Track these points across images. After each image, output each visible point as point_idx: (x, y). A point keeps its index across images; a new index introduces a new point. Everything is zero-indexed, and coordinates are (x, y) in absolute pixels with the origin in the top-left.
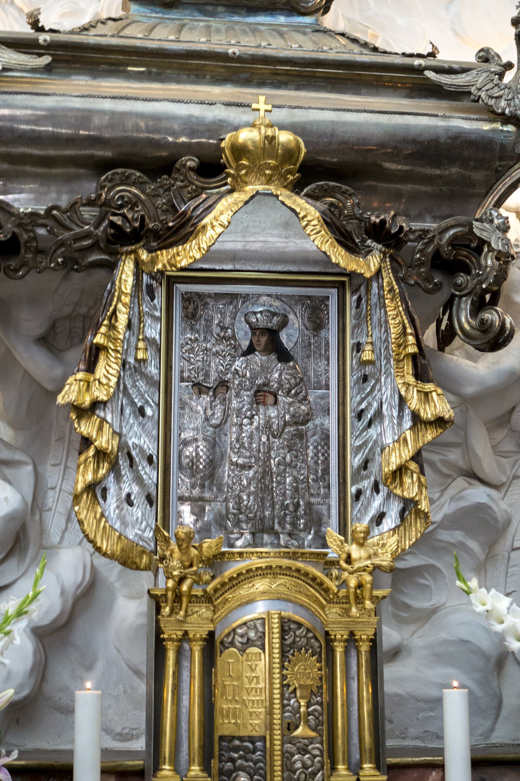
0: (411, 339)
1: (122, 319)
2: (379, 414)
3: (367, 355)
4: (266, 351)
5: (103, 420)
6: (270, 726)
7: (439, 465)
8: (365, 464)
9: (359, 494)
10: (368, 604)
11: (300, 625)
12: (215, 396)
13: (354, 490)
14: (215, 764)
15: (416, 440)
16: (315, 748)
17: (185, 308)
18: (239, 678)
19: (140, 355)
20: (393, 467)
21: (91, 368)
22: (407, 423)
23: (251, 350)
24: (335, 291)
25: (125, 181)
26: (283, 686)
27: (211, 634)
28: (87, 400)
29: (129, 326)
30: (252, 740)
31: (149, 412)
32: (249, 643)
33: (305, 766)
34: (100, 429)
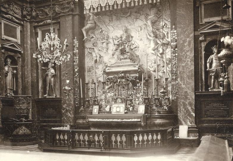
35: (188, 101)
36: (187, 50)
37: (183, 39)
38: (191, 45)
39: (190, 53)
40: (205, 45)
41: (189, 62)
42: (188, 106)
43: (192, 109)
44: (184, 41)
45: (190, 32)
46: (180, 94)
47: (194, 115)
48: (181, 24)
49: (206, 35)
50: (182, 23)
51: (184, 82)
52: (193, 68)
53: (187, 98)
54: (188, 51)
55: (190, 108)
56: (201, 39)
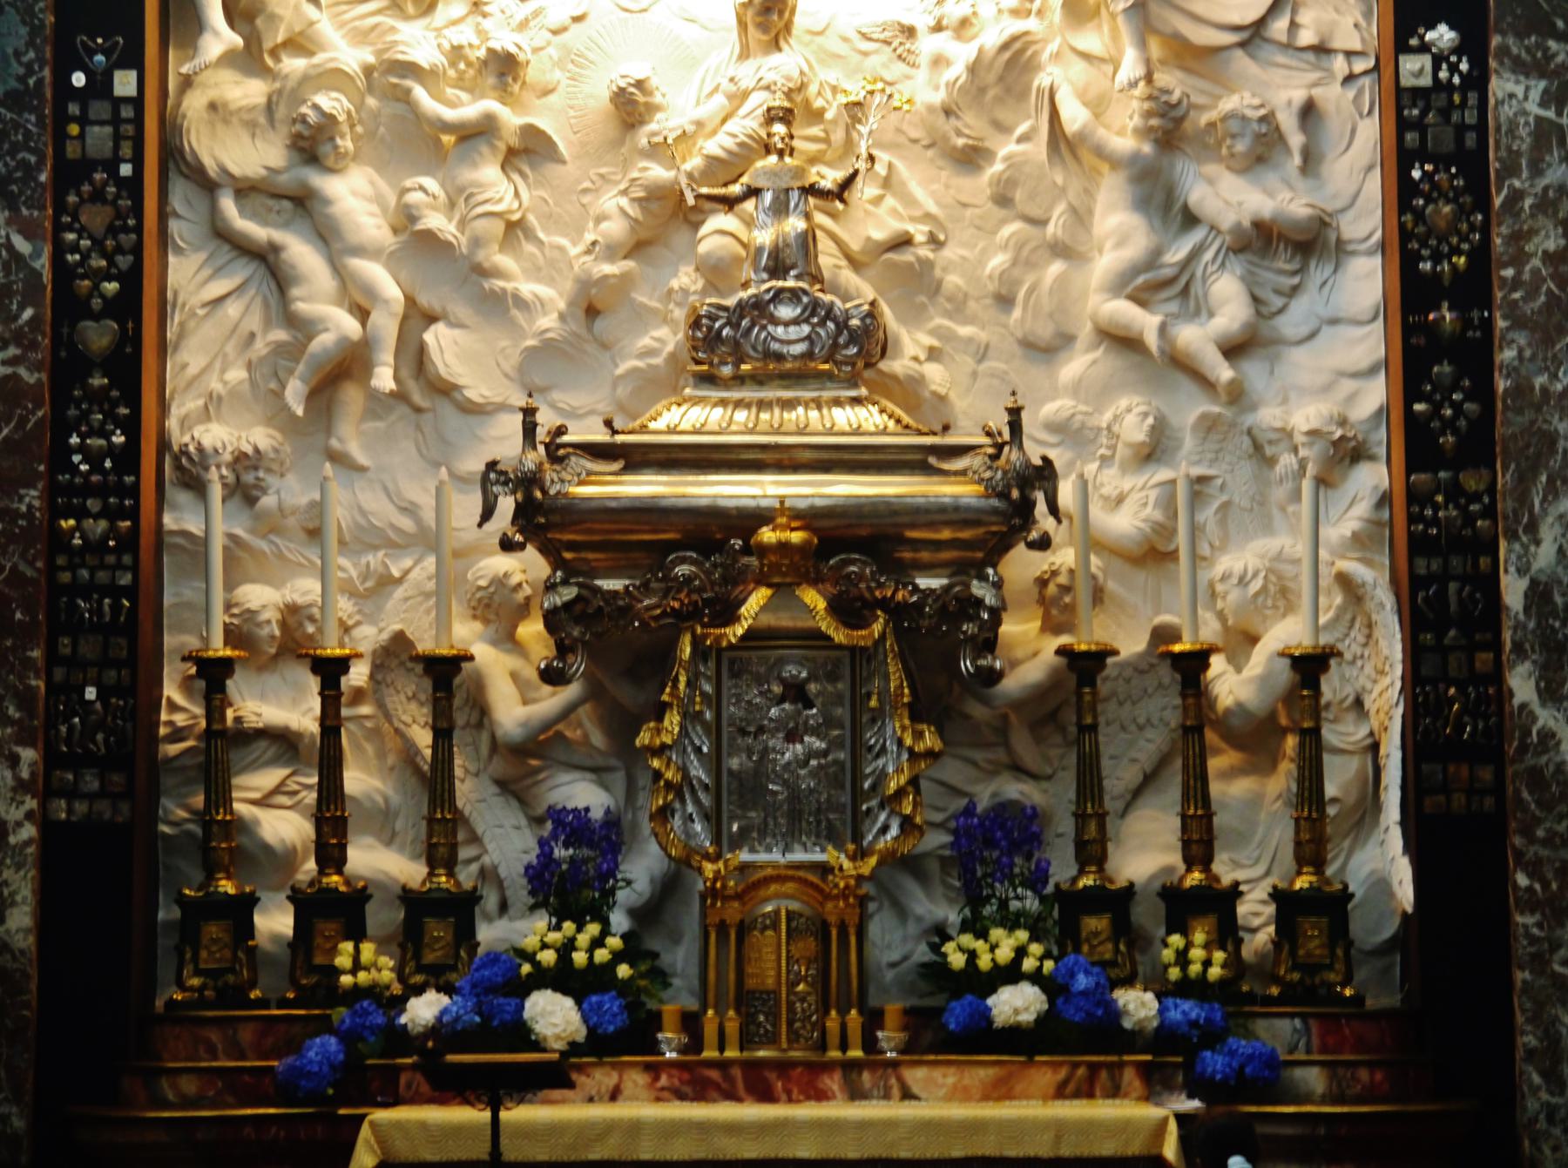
0: (906, 691)
1: (683, 679)
2: (884, 746)
3: (873, 703)
4: (793, 702)
5: (670, 759)
6: (779, 983)
7: (983, 764)
8: (874, 787)
9: (869, 810)
10: (851, 900)
11: (801, 915)
12: (755, 738)
13: (864, 807)
14: (743, 1009)
15: (911, 768)
16: (811, 999)
17: (731, 669)
18: (760, 951)
19: (697, 708)
20: (891, 792)
21: (660, 719)
22: (905, 756)
23: (781, 700)
24: (846, 653)
25: (683, 561)
26: (788, 958)
27: (742, 921)
28: (658, 742)
29: (688, 684)
30: (768, 993)
31: (705, 749)
32: (765, 928)
33: (803, 1010)
34: (668, 766)
46: (1544, 853)
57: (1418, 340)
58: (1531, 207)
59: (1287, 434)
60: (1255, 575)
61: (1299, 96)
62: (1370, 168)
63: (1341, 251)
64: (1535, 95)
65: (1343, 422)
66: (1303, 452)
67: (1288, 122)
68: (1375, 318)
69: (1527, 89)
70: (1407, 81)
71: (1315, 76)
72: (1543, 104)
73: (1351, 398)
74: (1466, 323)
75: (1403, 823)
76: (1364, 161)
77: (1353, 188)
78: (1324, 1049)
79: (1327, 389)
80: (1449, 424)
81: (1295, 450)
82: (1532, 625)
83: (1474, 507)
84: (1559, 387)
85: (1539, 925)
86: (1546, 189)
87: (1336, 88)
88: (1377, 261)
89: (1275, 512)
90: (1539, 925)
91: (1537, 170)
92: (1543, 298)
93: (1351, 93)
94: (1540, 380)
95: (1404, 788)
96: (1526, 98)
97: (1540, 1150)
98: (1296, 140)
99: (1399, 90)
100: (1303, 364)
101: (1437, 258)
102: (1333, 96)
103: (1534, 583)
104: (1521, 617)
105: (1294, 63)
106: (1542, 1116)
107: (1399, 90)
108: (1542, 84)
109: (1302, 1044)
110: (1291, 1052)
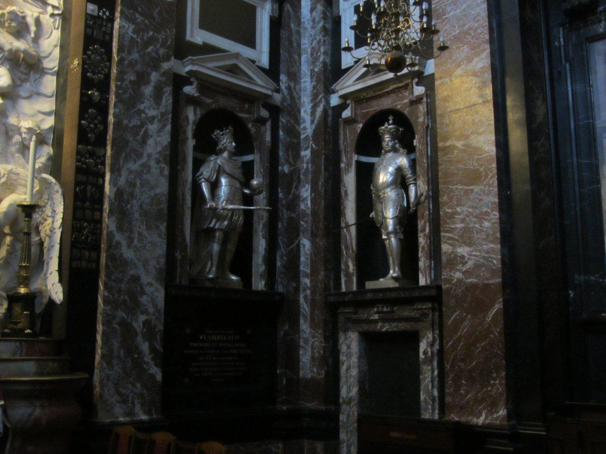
35: (143, 318)
36: (152, 113)
37: (138, 67)
38: (164, 101)
39: (160, 130)
40: (198, 117)
41: (152, 163)
42: (139, 339)
43: (153, 350)
44: (143, 78)
45: (162, 51)
47: (159, 377)
48: (137, 11)
49: (207, 85)
50: (140, 9)
51: (131, 240)
52: (163, 187)
53: (137, 304)
54: (153, 118)
55: (145, 347)
56: (189, 90)
57: (85, 99)
58: (127, 64)
59: (19, 129)
60: (4, 176)
61: (36, 15)
62: (56, 46)
63: (42, 72)
64: (131, 29)
65: (39, 128)
66: (24, 136)
67: (30, 21)
68: (52, 96)
69: (129, 26)
70: (89, 12)
71: (40, 10)
72: (133, 32)
73: (43, 120)
74: (102, 98)
75: (60, 271)
76: (55, 43)
77: (50, 51)
78: (28, 355)
79: (33, 116)
80: (92, 130)
81: (20, 134)
82: (116, 204)
83: (98, 161)
84: (131, 125)
85: (110, 310)
86: (132, 59)
87: (48, 16)
88: (55, 78)
89: (9, 155)
90: (110, 310)
91: (129, 53)
92: (128, 95)
93: (52, 20)
94: (125, 122)
95: (60, 258)
96: (128, 29)
97: (103, 390)
98: (33, 28)
99: (87, 14)
100: (26, 106)
101: (94, 73)
102: (46, 19)
103: (118, 190)
104: (113, 200)
105: (34, 3)
106: (106, 378)
107: (87, 14)
108: (133, 26)
109: (18, 353)
110: (14, 356)
